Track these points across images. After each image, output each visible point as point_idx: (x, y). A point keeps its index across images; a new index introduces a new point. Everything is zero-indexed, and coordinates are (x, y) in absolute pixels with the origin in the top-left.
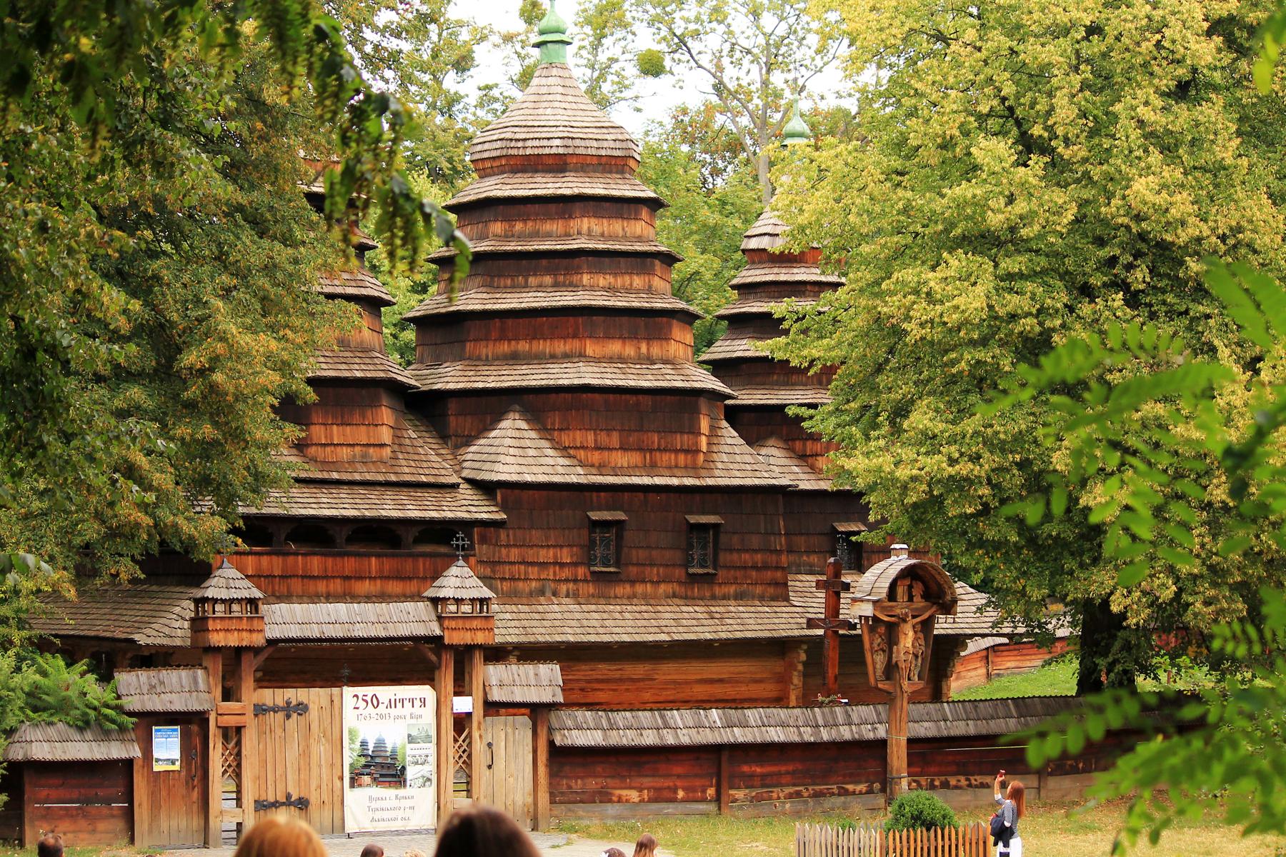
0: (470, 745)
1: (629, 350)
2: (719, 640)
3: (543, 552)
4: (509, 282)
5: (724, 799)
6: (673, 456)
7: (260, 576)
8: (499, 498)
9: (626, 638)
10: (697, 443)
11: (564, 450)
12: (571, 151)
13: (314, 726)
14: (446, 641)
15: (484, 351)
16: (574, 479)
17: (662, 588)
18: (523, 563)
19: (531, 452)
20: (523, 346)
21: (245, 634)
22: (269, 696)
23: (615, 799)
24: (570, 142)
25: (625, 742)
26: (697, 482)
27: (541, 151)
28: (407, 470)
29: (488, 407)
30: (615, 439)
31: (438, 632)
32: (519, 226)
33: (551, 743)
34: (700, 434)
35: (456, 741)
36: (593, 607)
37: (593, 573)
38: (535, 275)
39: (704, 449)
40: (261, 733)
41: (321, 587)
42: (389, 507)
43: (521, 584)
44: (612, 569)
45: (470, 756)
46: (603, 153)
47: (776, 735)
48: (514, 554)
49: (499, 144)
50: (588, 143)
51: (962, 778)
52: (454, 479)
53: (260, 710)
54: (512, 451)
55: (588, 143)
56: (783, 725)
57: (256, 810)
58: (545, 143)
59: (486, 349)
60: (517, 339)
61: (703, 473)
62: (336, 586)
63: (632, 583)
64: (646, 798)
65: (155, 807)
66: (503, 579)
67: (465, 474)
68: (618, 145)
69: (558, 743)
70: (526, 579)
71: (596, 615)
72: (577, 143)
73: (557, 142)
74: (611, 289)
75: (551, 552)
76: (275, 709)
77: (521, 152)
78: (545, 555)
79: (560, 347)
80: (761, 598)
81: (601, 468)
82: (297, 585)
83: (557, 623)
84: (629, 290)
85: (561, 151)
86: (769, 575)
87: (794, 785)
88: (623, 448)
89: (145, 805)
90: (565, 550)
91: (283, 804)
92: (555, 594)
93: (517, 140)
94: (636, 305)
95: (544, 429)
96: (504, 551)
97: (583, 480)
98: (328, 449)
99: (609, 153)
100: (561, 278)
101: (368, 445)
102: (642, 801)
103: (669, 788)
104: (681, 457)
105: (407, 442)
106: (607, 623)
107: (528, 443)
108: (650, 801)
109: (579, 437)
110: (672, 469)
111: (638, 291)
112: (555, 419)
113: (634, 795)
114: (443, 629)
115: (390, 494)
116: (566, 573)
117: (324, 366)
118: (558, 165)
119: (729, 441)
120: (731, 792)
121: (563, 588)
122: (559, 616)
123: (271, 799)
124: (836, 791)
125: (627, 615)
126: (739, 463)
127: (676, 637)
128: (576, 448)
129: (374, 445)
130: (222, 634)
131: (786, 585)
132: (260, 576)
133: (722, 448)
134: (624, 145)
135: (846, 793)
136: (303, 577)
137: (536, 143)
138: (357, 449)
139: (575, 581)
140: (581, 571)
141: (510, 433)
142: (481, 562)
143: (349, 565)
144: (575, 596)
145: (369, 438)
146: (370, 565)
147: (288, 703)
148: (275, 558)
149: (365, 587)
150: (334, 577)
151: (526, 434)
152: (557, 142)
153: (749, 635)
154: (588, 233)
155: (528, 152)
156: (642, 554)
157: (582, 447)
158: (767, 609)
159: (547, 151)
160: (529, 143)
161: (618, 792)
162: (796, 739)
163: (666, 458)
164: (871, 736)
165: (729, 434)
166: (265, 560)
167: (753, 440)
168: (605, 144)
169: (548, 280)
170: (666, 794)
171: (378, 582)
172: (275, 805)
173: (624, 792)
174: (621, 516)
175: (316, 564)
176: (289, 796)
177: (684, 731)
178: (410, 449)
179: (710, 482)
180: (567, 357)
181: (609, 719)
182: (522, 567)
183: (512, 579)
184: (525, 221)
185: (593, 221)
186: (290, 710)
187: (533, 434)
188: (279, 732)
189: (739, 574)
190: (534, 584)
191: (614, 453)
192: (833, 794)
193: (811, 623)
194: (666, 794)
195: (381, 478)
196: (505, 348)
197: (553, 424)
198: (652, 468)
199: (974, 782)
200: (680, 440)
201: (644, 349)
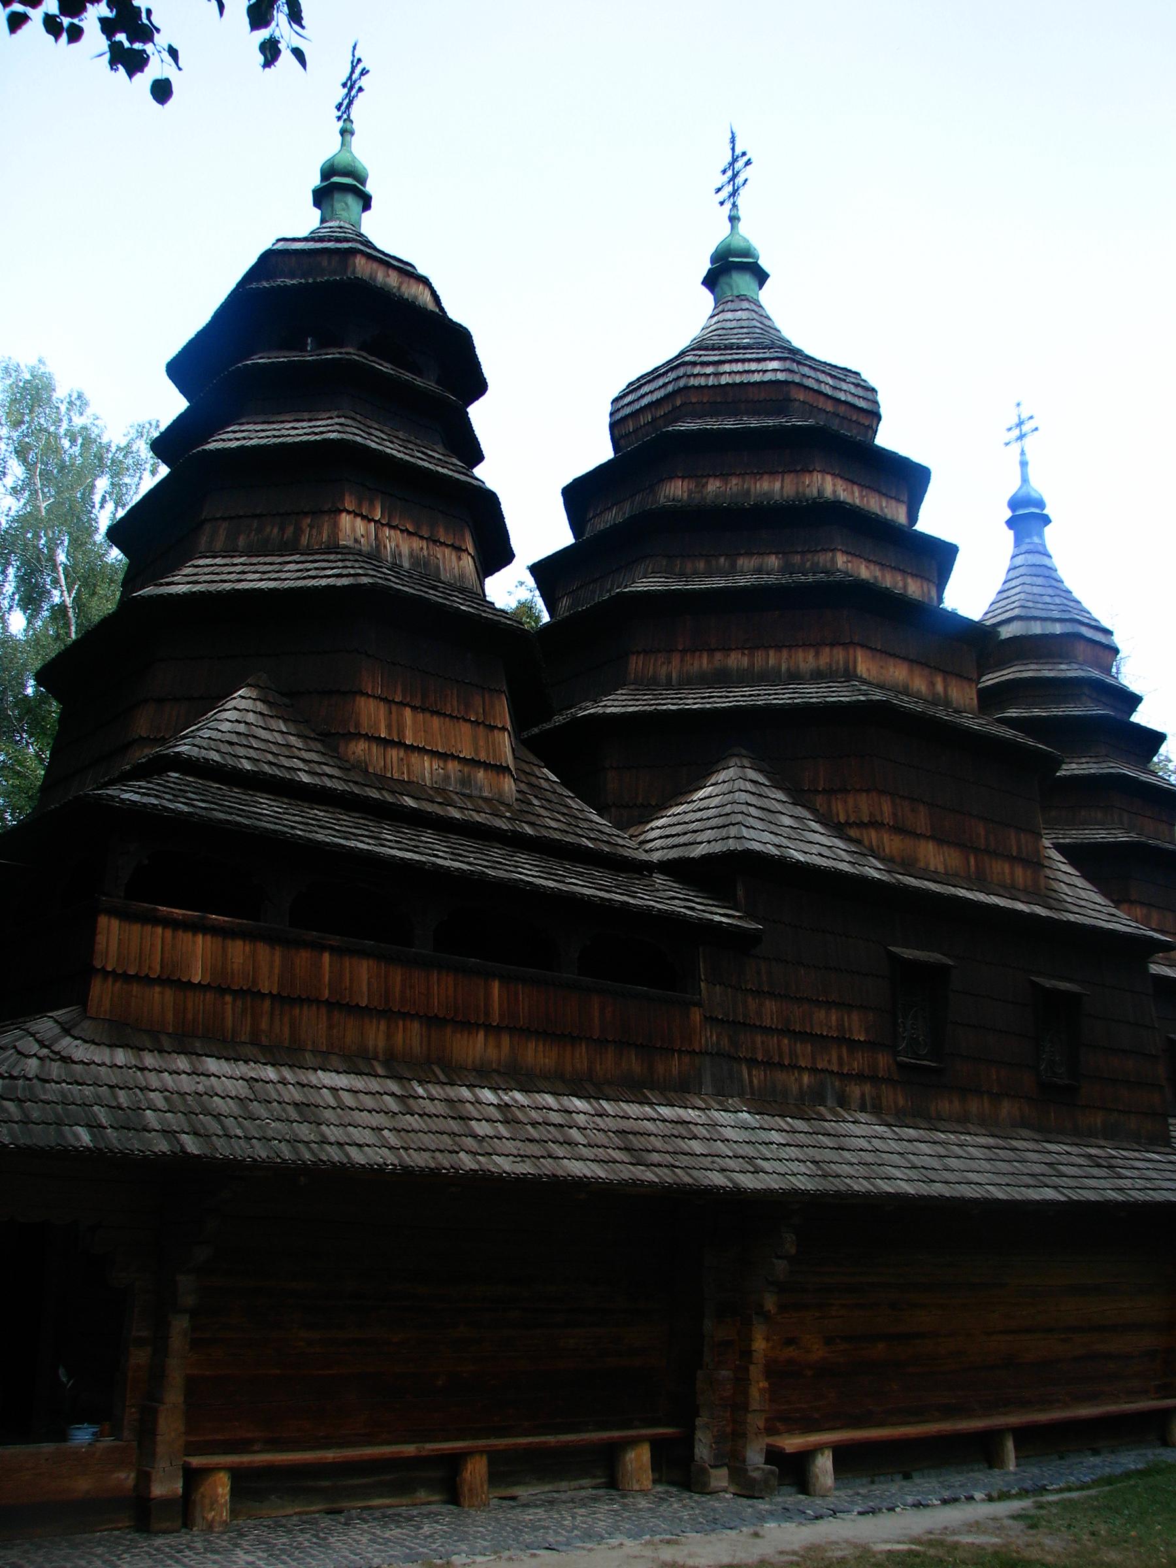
3: (820, 1015)
4: (701, 565)
7: (222, 991)
8: (740, 893)
11: (838, 829)
12: (797, 379)
15: (663, 671)
17: (1007, 1108)
18: (787, 1031)
20: (736, 660)
24: (794, 367)
27: (745, 378)
32: (713, 486)
37: (902, 1066)
38: (749, 554)
41: (376, 1035)
43: (781, 1076)
46: (842, 396)
49: (671, 376)
50: (822, 377)
54: (752, 810)
55: (822, 377)
58: (753, 366)
60: (727, 650)
62: (411, 1037)
66: (752, 1062)
68: (860, 392)
70: (794, 1067)
72: (806, 370)
77: (711, 381)
78: (826, 1021)
81: (908, 865)
82: (314, 1025)
85: (781, 376)
88: (940, 839)
90: (855, 1017)
92: (843, 1101)
93: (704, 364)
96: (752, 1004)
98: (394, 754)
99: (850, 399)
100: (797, 559)
101: (475, 763)
107: (779, 807)
109: (864, 805)
116: (858, 1063)
118: (776, 395)
121: (855, 1091)
126: (1084, 902)
128: (861, 825)
129: (487, 766)
132: (222, 991)
136: (329, 1004)
137: (739, 367)
138: (453, 766)
139: (874, 1079)
140: (883, 1061)
142: (710, 1019)
143: (441, 989)
145: (477, 751)
146: (488, 996)
148: (263, 950)
149: (476, 1047)
150: (405, 1016)
155: (724, 380)
159: (757, 378)
160: (727, 368)
163: (1000, 869)
166: (238, 950)
168: (844, 386)
169: (773, 561)
175: (363, 976)
183: (769, 1064)
184: (724, 476)
185: (839, 482)
187: (781, 796)
191: (923, 843)
196: (703, 663)
198: (980, 882)
201: (940, 687)
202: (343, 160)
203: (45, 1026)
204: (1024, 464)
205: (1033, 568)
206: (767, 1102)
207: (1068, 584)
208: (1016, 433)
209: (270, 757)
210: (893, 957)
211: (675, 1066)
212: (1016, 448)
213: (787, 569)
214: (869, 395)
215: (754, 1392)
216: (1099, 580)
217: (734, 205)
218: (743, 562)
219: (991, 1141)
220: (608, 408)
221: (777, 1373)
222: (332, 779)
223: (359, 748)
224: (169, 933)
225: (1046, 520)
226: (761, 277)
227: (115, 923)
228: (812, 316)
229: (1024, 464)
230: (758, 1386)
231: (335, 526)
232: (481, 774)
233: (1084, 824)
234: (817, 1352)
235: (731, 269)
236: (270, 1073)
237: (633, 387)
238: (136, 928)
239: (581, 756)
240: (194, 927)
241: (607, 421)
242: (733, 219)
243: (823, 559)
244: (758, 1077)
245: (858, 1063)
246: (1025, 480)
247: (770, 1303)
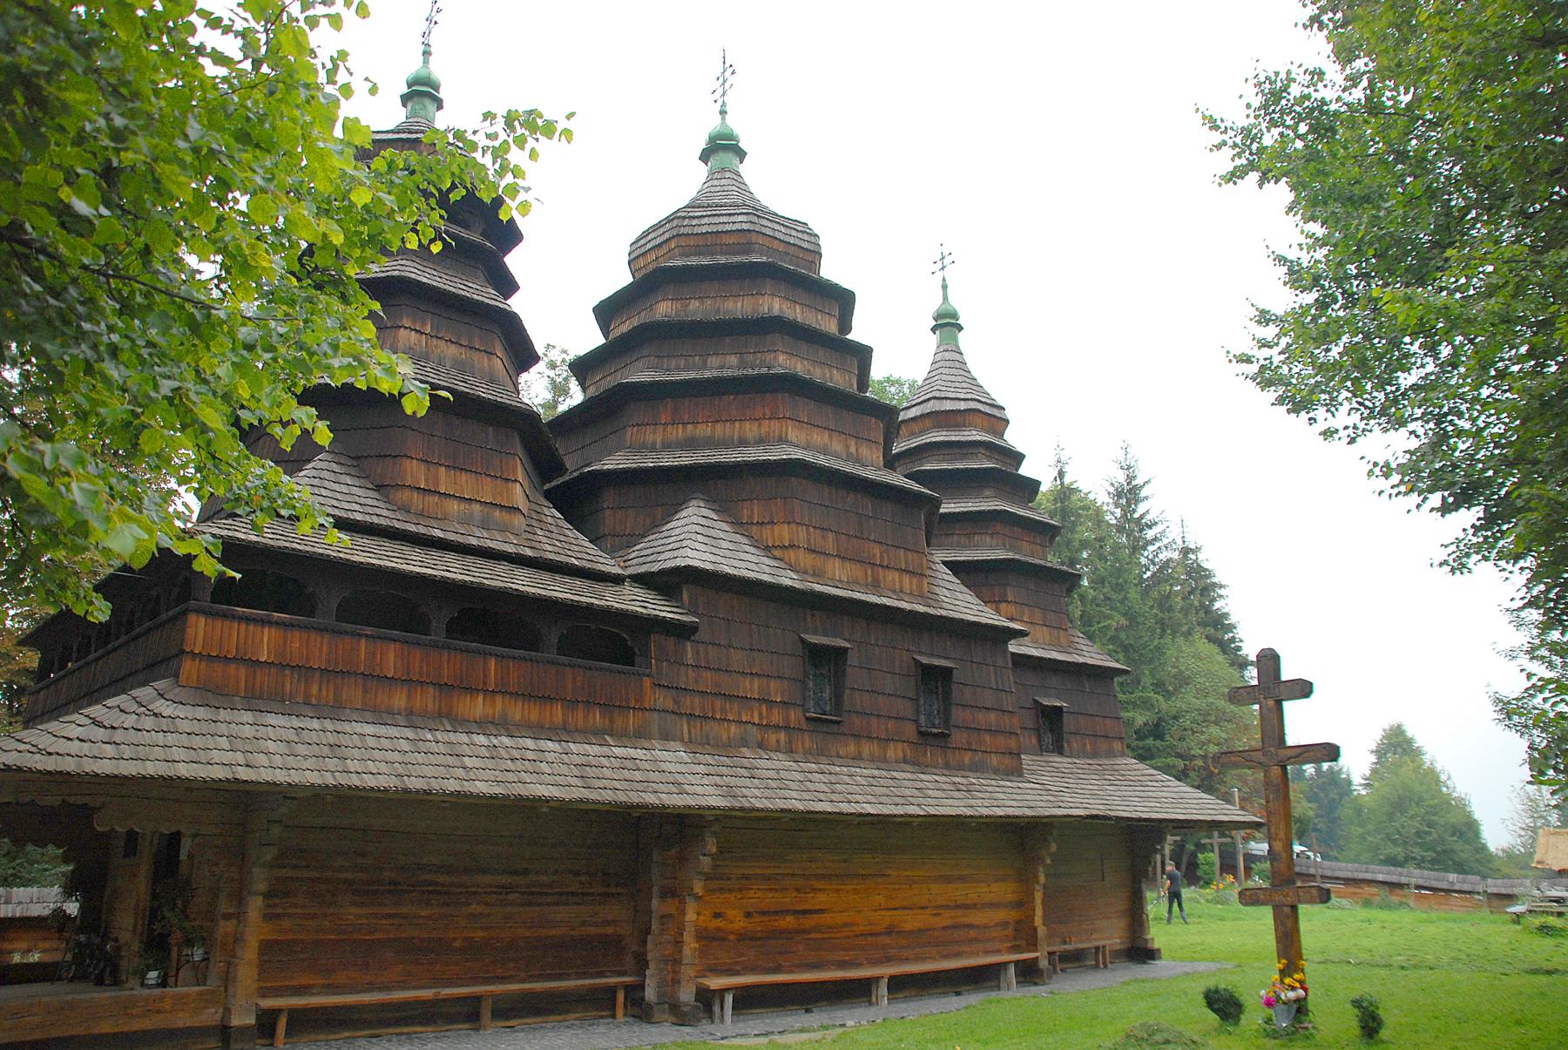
6: (897, 575)
8: (685, 596)
9: (870, 809)
11: (767, 549)
16: (788, 582)
17: (893, 752)
19: (725, 544)
20: (703, 430)
24: (755, 219)
26: (931, 611)
27: (720, 228)
29: (665, 489)
30: (831, 547)
32: (694, 305)
41: (399, 700)
42: (524, 582)
48: (707, 680)
50: (776, 227)
54: (700, 538)
55: (776, 227)
59: (654, 436)
68: (806, 237)
73: (740, 218)
78: (751, 687)
79: (751, 430)
80: (996, 771)
81: (818, 574)
82: (352, 692)
85: (745, 226)
86: (1002, 741)
90: (773, 684)
95: (739, 525)
97: (797, 585)
104: (906, 578)
107: (722, 535)
109: (784, 533)
110: (899, 593)
112: (754, 511)
116: (777, 717)
121: (772, 738)
126: (961, 603)
127: (932, 811)
138: (477, 508)
139: (787, 728)
140: (795, 716)
141: (695, 519)
144: (790, 751)
146: (486, 669)
148: (314, 637)
149: (478, 707)
151: (715, 524)
153: (1000, 812)
157: (791, 546)
163: (892, 576)
169: (733, 360)
171: (499, 699)
175: (391, 658)
180: (760, 441)
182: (718, 703)
187: (725, 526)
191: (831, 561)
195: (510, 549)
197: (751, 517)
198: (875, 586)
201: (853, 450)
202: (424, 73)
203: (144, 693)
204: (945, 287)
205: (950, 359)
206: (695, 745)
207: (975, 374)
208: (939, 265)
209: (335, 503)
210: (803, 641)
211: (632, 720)
212: (939, 275)
213: (743, 365)
214: (813, 239)
215: (687, 951)
216: (995, 369)
217: (724, 104)
218: (713, 361)
220: (628, 249)
221: (707, 937)
222: (382, 515)
223: (403, 496)
224: (243, 626)
225: (960, 328)
226: (741, 155)
227: (202, 620)
228: (777, 185)
229: (945, 287)
230: (690, 945)
232: (497, 513)
233: (976, 547)
234: (739, 923)
235: (722, 148)
236: (315, 724)
237: (645, 234)
238: (219, 623)
239: (577, 500)
240: (263, 622)
241: (627, 258)
242: (723, 112)
243: (769, 357)
245: (777, 717)
246: (945, 298)
247: (698, 888)
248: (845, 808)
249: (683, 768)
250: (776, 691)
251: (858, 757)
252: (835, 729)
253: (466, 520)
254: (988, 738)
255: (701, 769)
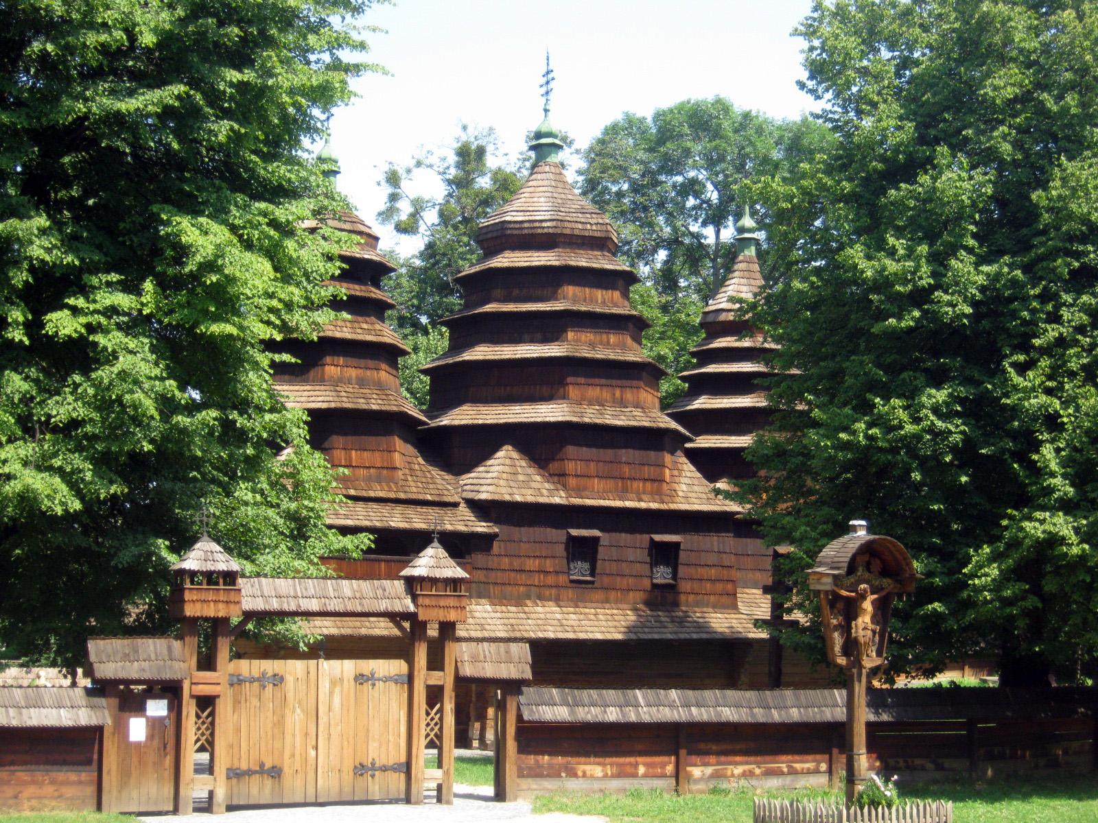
0: (441, 719)
1: (606, 394)
2: (679, 640)
5: (681, 775)
9: (599, 636)
10: (663, 474)
13: (290, 695)
14: (421, 618)
21: (221, 606)
22: (246, 667)
23: (580, 773)
25: (589, 718)
28: (414, 490)
31: (412, 608)
33: (520, 718)
34: (664, 466)
35: (428, 714)
36: (571, 610)
37: (572, 581)
39: (668, 478)
40: (237, 702)
43: (509, 588)
44: (589, 578)
45: (441, 729)
47: (729, 714)
48: (505, 562)
51: (901, 761)
52: (456, 499)
53: (237, 681)
55: (573, 225)
56: (737, 706)
57: (228, 778)
61: (666, 499)
63: (606, 589)
64: (609, 773)
65: (125, 774)
67: (465, 495)
68: (599, 227)
69: (526, 717)
71: (573, 616)
73: (548, 224)
74: (592, 345)
75: (537, 561)
76: (252, 680)
78: (532, 564)
83: (540, 622)
84: (607, 344)
85: (551, 231)
86: (719, 587)
87: (747, 763)
89: (114, 772)
90: (548, 561)
91: (256, 772)
94: (612, 357)
102: (605, 776)
103: (630, 764)
104: (648, 485)
105: (417, 467)
106: (583, 622)
108: (613, 776)
111: (614, 347)
113: (598, 771)
114: (416, 605)
115: (399, 509)
116: (550, 580)
117: (345, 399)
119: (689, 474)
120: (689, 769)
122: (542, 616)
123: (244, 766)
124: (785, 770)
125: (601, 617)
130: (198, 605)
131: (735, 595)
133: (682, 480)
134: (604, 228)
135: (793, 772)
139: (557, 586)
140: (562, 579)
144: (557, 601)
146: (380, 568)
147: (264, 674)
152: (548, 224)
154: (570, 299)
156: (614, 567)
158: (719, 615)
159: (539, 231)
161: (582, 767)
162: (750, 720)
163: (635, 484)
164: (818, 719)
165: (688, 469)
167: (711, 476)
168: (589, 227)
170: (629, 769)
172: (249, 773)
173: (588, 768)
174: (596, 533)
176: (262, 765)
177: (645, 709)
178: (419, 473)
179: (673, 506)
181: (574, 698)
182: (513, 574)
186: (262, 680)
187: (523, 463)
188: (255, 702)
189: (696, 585)
190: (521, 588)
191: (592, 479)
192: (782, 773)
193: (758, 623)
194: (629, 769)
195: (392, 495)
198: (623, 493)
199: (910, 764)
200: (647, 471)
219: (615, 611)
231: (323, 371)
232: (385, 472)
244: (497, 589)
248: (582, 636)
249: (485, 615)
250: (549, 565)
251: (607, 601)
252: (590, 586)
253: (369, 479)
254: (708, 585)
255: (499, 615)
